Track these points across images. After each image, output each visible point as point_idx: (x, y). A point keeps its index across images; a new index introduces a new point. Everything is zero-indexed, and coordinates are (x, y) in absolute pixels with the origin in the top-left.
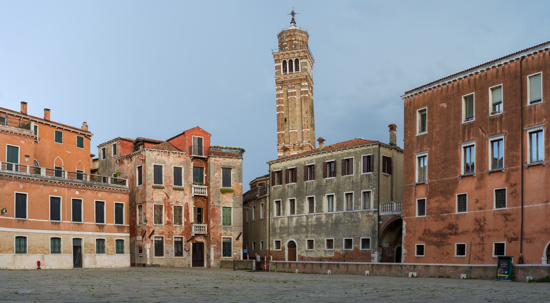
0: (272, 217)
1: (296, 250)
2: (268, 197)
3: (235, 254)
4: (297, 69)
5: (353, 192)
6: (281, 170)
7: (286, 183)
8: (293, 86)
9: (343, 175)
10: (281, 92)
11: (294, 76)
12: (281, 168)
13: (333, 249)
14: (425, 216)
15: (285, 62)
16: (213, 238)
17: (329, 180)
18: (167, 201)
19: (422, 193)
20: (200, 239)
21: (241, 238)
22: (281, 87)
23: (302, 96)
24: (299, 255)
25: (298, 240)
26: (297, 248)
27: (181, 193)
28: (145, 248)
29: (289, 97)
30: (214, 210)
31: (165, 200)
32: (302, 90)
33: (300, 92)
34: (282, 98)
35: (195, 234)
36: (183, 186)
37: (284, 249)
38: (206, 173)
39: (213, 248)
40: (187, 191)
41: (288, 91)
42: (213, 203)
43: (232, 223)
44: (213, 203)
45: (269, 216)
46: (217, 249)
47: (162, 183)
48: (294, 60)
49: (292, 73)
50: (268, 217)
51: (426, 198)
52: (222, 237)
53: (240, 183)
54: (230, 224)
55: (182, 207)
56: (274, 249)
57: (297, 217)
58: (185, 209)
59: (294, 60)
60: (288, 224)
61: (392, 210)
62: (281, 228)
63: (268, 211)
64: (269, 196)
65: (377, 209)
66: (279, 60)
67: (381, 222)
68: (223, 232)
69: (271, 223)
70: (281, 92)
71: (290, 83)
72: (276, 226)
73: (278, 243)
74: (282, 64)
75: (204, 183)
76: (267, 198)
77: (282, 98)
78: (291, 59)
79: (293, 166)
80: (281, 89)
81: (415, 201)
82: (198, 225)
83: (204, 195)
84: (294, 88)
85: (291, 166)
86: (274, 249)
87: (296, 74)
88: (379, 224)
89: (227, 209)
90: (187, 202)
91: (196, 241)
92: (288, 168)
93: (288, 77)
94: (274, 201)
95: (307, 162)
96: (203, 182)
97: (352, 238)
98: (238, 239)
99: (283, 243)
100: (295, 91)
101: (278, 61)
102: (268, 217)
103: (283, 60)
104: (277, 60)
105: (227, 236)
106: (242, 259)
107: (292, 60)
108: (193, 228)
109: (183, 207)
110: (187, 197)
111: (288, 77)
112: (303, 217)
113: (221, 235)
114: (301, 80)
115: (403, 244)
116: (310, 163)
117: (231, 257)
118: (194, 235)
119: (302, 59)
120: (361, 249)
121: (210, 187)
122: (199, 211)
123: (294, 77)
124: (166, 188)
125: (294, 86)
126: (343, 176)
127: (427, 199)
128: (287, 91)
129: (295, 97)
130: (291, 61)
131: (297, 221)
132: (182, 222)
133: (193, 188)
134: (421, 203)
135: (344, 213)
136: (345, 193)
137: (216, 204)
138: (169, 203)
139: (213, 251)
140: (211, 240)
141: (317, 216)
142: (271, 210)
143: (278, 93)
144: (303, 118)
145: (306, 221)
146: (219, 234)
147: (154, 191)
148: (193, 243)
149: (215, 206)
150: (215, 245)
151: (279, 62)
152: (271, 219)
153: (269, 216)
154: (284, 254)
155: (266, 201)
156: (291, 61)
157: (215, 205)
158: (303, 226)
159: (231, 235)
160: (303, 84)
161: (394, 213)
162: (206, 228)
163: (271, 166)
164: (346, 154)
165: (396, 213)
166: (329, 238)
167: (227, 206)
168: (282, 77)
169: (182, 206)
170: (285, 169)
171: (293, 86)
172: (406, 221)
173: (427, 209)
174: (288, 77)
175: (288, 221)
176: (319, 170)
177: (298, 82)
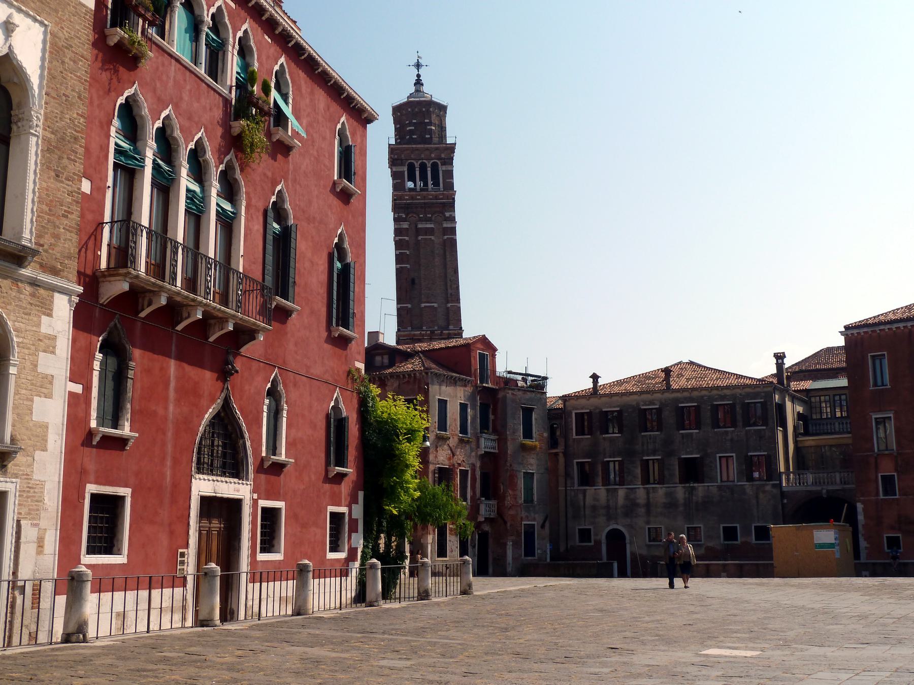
0: (572, 488)
1: (626, 544)
2: (561, 455)
3: (539, 551)
4: (436, 183)
5: (734, 455)
6: (588, 411)
7: (602, 433)
8: (428, 215)
9: (713, 428)
10: (405, 225)
11: (431, 197)
12: (588, 409)
13: (702, 542)
14: (897, 497)
15: (411, 168)
16: (511, 525)
17: (687, 434)
18: (451, 461)
19: (887, 469)
20: (486, 528)
21: (547, 524)
22: (404, 216)
23: (446, 237)
24: (632, 554)
25: (630, 527)
26: (627, 541)
27: (468, 447)
28: (422, 542)
29: (420, 238)
30: (513, 477)
31: (449, 459)
32: (445, 225)
33: (441, 230)
34: (407, 238)
35: (485, 518)
36: (469, 436)
37: (598, 543)
38: (494, 413)
39: (511, 543)
40: (474, 445)
41: (420, 226)
42: (511, 465)
43: (535, 499)
44: (511, 465)
45: (566, 487)
46: (516, 544)
47: (446, 431)
48: (429, 165)
49: (427, 190)
50: (564, 488)
51: (895, 474)
52: (524, 523)
53: (545, 434)
54: (532, 501)
55: (468, 470)
56: (578, 543)
57: (626, 490)
58: (471, 475)
59: (429, 165)
60: (608, 500)
61: (803, 484)
62: (594, 508)
63: (561, 480)
64: (565, 454)
65: (778, 482)
66: (402, 160)
67: (785, 501)
68: (524, 514)
69: (569, 498)
70: (405, 225)
71: (423, 210)
72: (582, 503)
73: (585, 535)
74: (405, 169)
75: (491, 430)
76: (558, 455)
77: (407, 238)
78: (424, 161)
79: (615, 407)
80: (405, 220)
81: (877, 477)
82: (488, 502)
83: (492, 451)
84: (429, 220)
85: (611, 407)
86: (577, 542)
87: (433, 193)
88: (783, 505)
89: (529, 476)
90: (474, 462)
91: (483, 529)
92: (604, 410)
93: (418, 197)
94: (575, 461)
95: (642, 403)
96: (488, 429)
97: (738, 525)
98: (543, 526)
99: (596, 535)
100: (432, 226)
101: (399, 162)
102: (561, 488)
103: (409, 161)
104: (397, 160)
105: (529, 521)
106: (548, 560)
107: (426, 165)
108: (483, 508)
109: (470, 471)
110: (473, 454)
111: (419, 197)
112: (637, 490)
113: (522, 519)
114: (444, 204)
115: (860, 536)
116: (649, 405)
117: (534, 558)
118: (483, 519)
119: (444, 164)
120: (754, 541)
121: (506, 440)
122: (484, 476)
123: (431, 199)
124: (451, 438)
125: (430, 216)
126: (714, 429)
127: (898, 475)
128: (416, 226)
129: (433, 238)
130: (423, 168)
131: (627, 497)
132: (466, 496)
133: (482, 441)
134: (888, 482)
135: (719, 487)
136: (718, 455)
137: (515, 467)
138: (454, 465)
139: (511, 547)
140: (509, 528)
141: (668, 489)
142: (568, 475)
143: (399, 227)
144: (449, 284)
145: (646, 497)
146: (519, 519)
147: (438, 443)
148: (479, 534)
149: (513, 470)
150: (513, 538)
151: (402, 164)
152: (568, 492)
153: (566, 487)
154: (600, 551)
155: (558, 460)
156: (423, 168)
157: (514, 469)
158: (637, 505)
159: (534, 520)
160: (447, 214)
161: (809, 488)
162: (496, 507)
163: (567, 403)
164: (717, 397)
165: (814, 488)
166: (693, 524)
167: (529, 471)
168: (406, 195)
169: (469, 469)
170: (597, 411)
171: (428, 215)
172: (863, 502)
173: (899, 489)
174: (419, 197)
175: (607, 496)
176: (669, 417)
177: (438, 209)
